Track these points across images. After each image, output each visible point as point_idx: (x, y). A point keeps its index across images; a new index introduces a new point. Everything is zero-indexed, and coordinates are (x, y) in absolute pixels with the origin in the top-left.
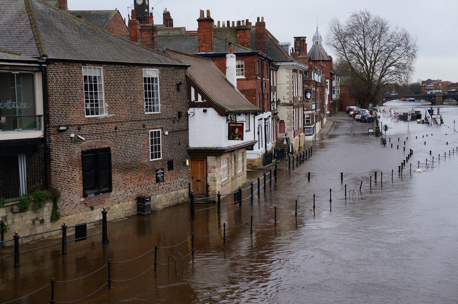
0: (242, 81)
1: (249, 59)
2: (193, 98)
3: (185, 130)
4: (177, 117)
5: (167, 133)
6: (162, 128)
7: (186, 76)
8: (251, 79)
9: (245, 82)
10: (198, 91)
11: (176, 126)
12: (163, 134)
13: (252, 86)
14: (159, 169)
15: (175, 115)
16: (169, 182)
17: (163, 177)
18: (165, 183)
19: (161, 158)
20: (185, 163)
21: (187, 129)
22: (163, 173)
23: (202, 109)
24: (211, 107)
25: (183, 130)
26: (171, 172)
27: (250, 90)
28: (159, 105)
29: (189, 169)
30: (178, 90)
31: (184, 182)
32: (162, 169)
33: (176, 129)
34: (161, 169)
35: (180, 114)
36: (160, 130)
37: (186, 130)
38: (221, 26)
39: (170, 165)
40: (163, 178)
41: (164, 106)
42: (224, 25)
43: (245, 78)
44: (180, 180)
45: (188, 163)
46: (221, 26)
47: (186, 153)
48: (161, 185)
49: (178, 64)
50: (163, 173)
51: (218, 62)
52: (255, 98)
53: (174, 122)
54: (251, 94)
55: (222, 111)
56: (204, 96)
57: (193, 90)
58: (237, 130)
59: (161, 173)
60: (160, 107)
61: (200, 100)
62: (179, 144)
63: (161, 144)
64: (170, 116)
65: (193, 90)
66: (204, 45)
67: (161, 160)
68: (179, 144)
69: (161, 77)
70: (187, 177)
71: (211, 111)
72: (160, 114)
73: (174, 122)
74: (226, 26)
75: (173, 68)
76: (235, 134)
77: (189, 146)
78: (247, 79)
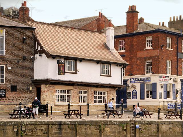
0: (151, 51)
1: (155, 35)
2: (36, 48)
3: (31, 68)
4: (22, 59)
5: (10, 68)
6: (6, 65)
7: (33, 35)
8: (156, 49)
9: (152, 51)
10: (39, 44)
11: (20, 65)
12: (7, 68)
13: (157, 53)
14: (1, 90)
15: (20, 57)
16: (12, 98)
17: (5, 95)
18: (7, 99)
19: (4, 83)
20: (29, 88)
21: (33, 68)
22: (4, 92)
23: (38, 55)
24: (43, 53)
25: (28, 68)
26: (14, 92)
27: (155, 56)
28: (5, 50)
29: (34, 93)
30: (24, 43)
31: (27, 100)
32: (5, 90)
33: (20, 67)
34: (3, 90)
35: (24, 59)
36: (4, 66)
37: (32, 68)
38: (176, 20)
39: (14, 88)
40: (5, 95)
41: (9, 52)
42: (177, 19)
43: (152, 48)
44: (24, 99)
45: (31, 89)
46: (176, 20)
47: (30, 83)
48: (3, 100)
49: (30, 27)
50: (4, 92)
51: (136, 38)
52: (158, 62)
53: (18, 62)
54: (156, 59)
55: (50, 56)
56: (41, 47)
57: (36, 43)
58: (62, 68)
59: (3, 92)
60: (5, 51)
61: (39, 49)
62: (24, 76)
63: (4, 74)
64: (15, 58)
65: (36, 43)
66: (130, 28)
67: (4, 84)
68: (24, 76)
69: (7, 34)
70: (30, 98)
71: (44, 55)
72: (4, 56)
73: (18, 62)
74: (179, 19)
75: (19, 29)
76: (61, 71)
77: (33, 78)
78: (153, 49)
